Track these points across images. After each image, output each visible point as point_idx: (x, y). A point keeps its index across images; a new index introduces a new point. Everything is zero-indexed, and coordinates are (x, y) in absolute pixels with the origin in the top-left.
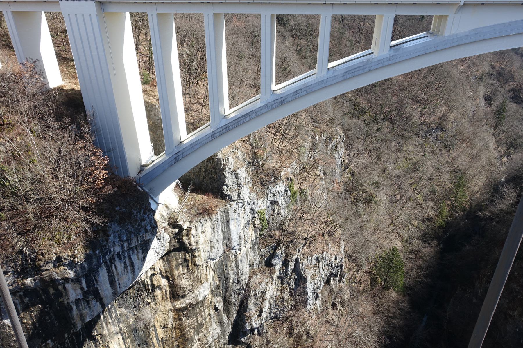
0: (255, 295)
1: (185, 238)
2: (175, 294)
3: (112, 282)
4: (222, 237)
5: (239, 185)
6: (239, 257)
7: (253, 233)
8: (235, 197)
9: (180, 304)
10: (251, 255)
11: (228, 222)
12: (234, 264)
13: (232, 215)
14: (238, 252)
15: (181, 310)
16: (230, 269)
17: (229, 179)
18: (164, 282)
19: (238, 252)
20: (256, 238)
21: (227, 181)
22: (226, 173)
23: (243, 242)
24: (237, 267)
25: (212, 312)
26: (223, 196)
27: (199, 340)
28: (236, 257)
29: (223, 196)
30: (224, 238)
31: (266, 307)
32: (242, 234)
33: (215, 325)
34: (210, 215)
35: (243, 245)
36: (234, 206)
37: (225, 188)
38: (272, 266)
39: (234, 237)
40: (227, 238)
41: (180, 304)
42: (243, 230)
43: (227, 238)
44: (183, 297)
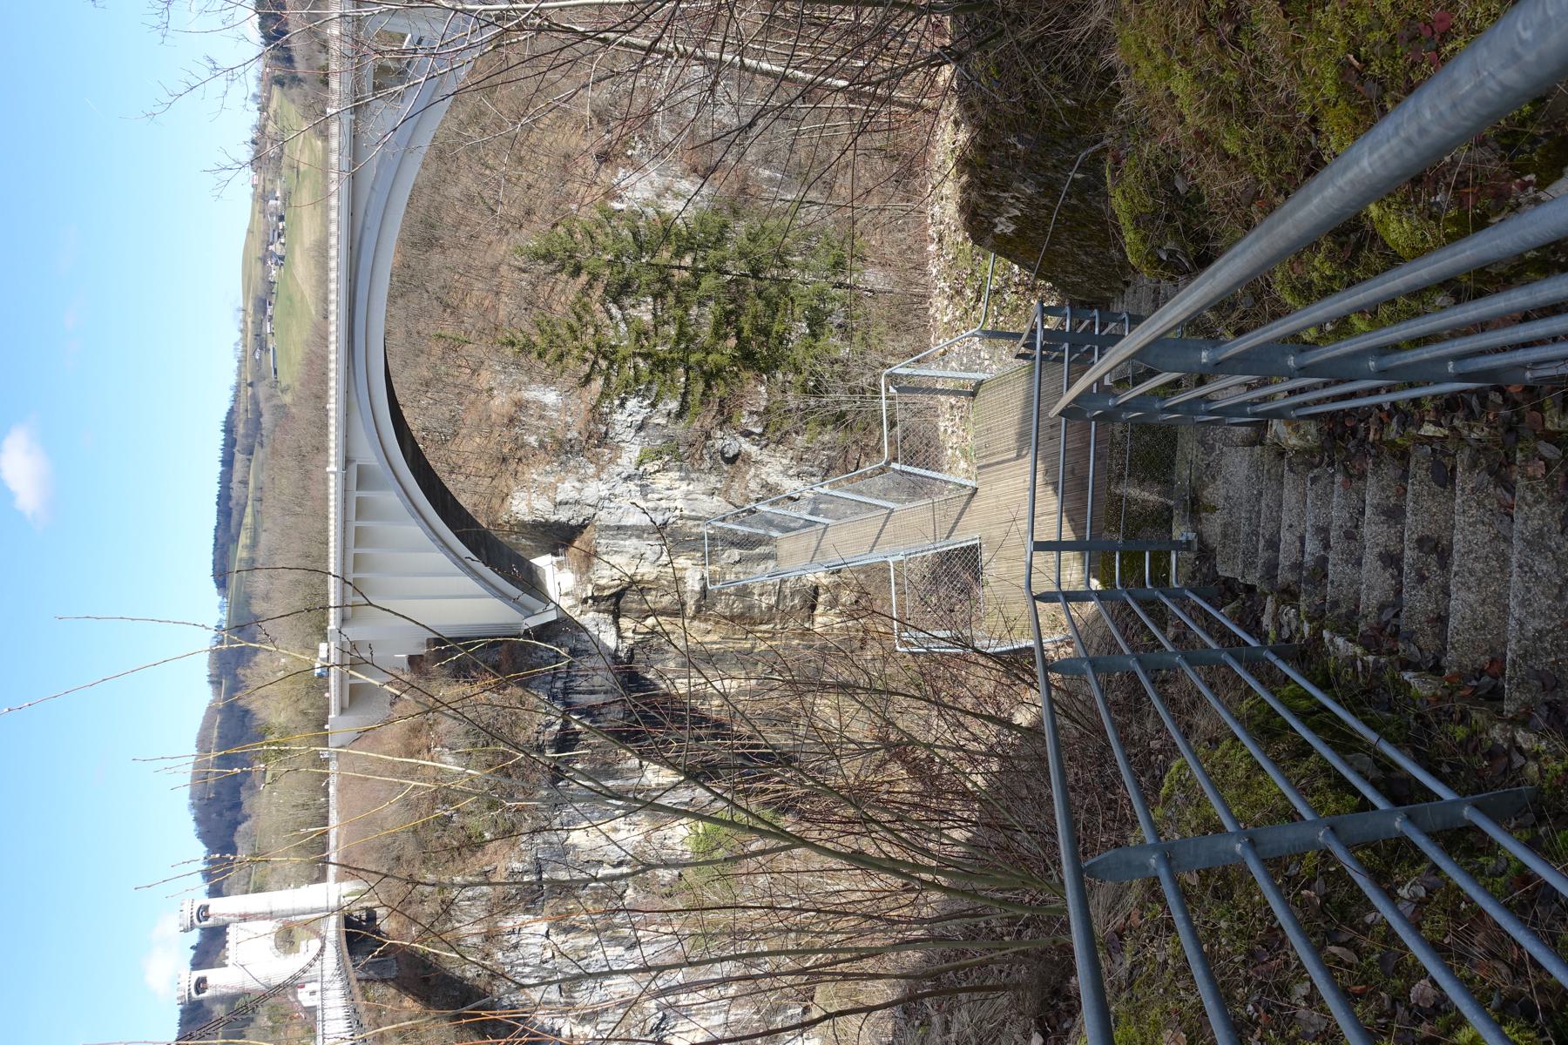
0: (758, 500)
1: (606, 593)
2: (677, 611)
3: (592, 693)
4: (634, 541)
5: (577, 502)
6: (686, 512)
7: (671, 474)
8: (591, 511)
9: (690, 610)
10: (701, 487)
11: (619, 528)
12: (690, 523)
13: (613, 521)
14: (678, 513)
15: (699, 609)
16: (694, 530)
17: (563, 516)
18: (651, 621)
19: (678, 513)
20: (680, 469)
21: (564, 519)
22: (553, 518)
23: (664, 504)
24: (699, 519)
25: (738, 568)
26: (582, 527)
27: (761, 595)
28: (682, 518)
29: (582, 527)
30: (639, 537)
31: (791, 486)
32: (651, 505)
33: (762, 566)
34: (596, 554)
35: (672, 505)
36: (602, 514)
37: (573, 522)
38: (736, 457)
39: (644, 520)
40: (638, 532)
41: (690, 610)
42: (647, 501)
43: (638, 532)
44: (683, 604)
